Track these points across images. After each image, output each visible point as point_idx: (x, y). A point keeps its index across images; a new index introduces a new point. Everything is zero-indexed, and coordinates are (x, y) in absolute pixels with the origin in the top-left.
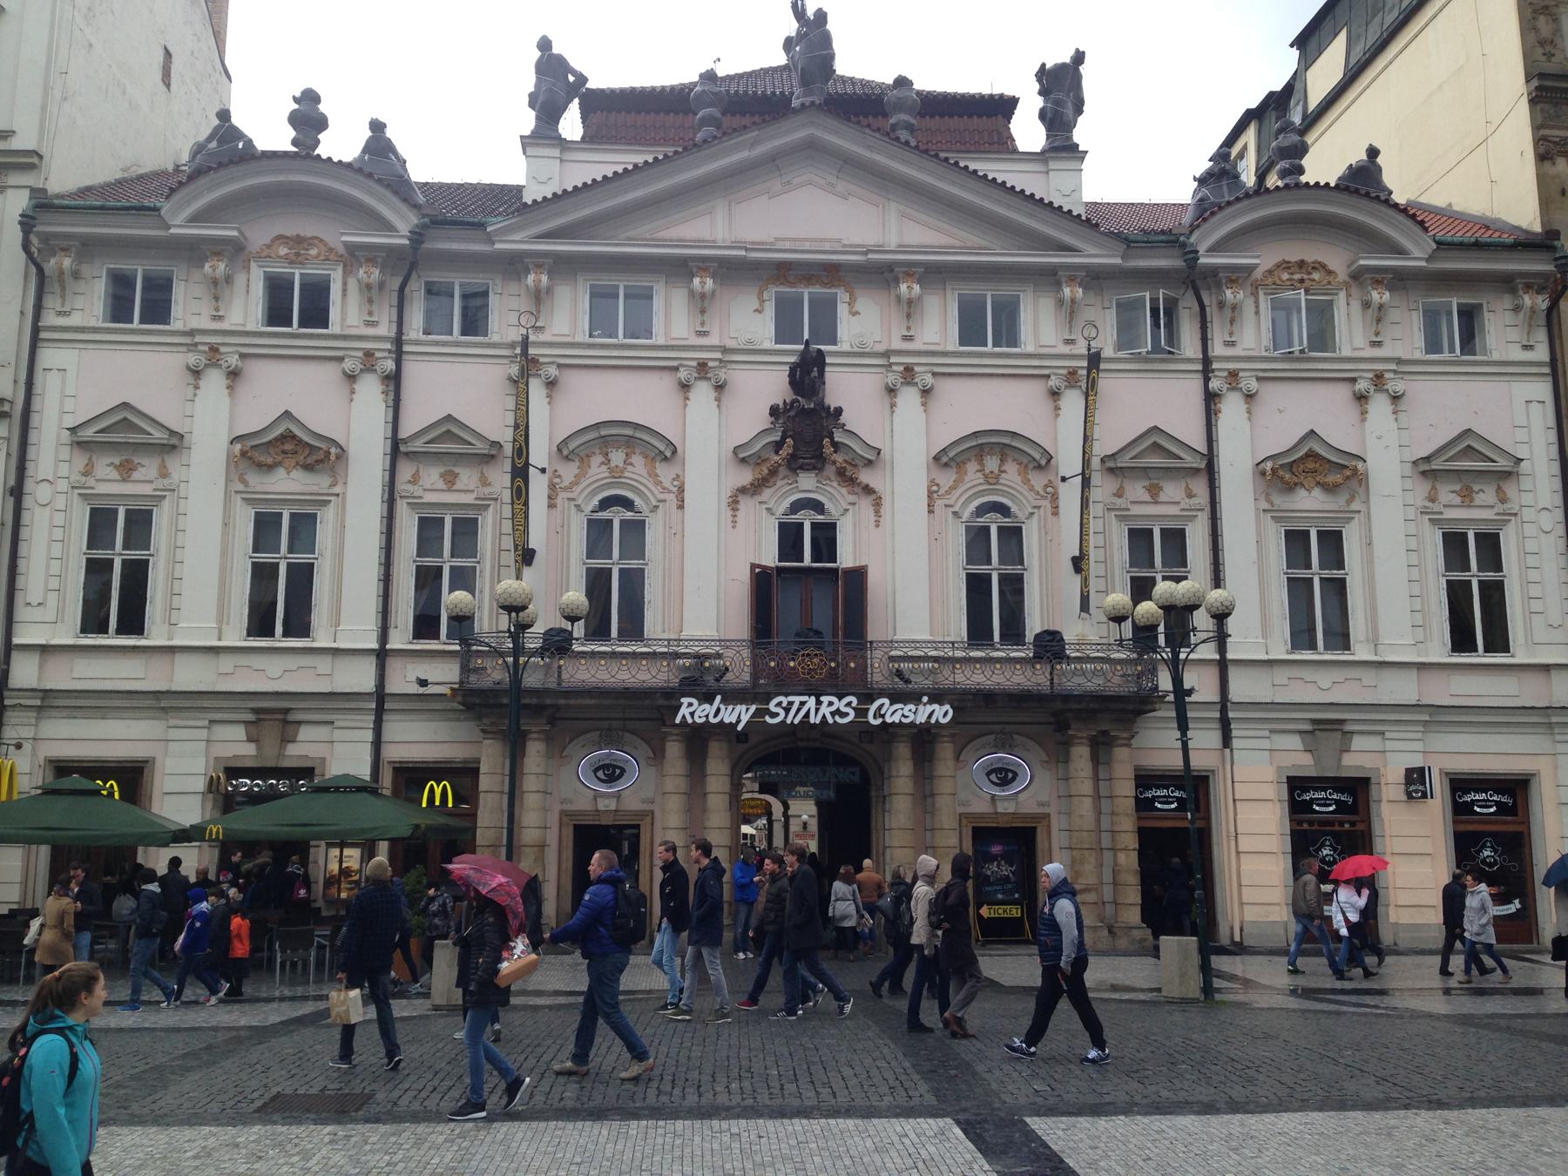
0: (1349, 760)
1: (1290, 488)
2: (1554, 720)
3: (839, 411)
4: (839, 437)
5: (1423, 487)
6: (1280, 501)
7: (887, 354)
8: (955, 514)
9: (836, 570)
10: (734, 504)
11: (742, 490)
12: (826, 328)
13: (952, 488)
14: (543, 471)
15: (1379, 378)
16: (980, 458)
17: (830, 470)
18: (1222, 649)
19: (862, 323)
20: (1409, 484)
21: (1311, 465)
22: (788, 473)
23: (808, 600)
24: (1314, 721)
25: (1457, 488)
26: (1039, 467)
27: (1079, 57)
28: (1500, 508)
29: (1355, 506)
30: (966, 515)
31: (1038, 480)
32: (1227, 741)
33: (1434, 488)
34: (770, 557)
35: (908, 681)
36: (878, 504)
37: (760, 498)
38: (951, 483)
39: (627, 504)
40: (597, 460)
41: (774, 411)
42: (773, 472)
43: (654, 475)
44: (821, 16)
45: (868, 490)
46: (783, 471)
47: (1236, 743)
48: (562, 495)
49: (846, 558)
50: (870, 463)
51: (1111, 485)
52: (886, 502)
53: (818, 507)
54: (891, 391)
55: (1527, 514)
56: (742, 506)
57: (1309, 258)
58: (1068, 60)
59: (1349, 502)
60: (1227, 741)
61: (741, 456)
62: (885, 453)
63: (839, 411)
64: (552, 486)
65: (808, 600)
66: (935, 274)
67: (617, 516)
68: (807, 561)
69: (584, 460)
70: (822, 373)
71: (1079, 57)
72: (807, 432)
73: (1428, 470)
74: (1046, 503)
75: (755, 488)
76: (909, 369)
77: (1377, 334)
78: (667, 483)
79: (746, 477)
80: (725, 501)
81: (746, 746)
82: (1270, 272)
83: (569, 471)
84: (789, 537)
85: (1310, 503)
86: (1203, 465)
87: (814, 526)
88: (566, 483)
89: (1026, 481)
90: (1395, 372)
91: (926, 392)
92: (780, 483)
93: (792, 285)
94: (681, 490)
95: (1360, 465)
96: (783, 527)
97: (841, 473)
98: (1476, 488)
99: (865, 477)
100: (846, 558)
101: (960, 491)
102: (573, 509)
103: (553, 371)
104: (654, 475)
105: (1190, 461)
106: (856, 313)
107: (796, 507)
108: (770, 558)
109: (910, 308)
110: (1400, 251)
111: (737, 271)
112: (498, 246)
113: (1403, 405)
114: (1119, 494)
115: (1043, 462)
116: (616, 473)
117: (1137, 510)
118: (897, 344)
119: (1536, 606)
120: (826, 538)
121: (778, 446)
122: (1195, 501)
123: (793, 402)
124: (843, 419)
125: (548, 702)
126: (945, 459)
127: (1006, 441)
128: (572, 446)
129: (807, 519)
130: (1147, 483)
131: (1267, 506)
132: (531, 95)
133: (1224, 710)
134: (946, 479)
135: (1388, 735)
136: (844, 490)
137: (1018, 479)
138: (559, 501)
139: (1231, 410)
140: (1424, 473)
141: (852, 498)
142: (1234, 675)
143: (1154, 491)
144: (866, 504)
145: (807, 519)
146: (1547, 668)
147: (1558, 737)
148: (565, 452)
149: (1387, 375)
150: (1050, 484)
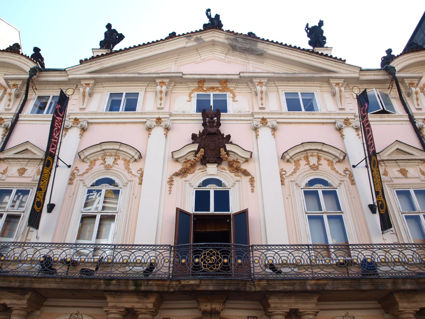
3: (229, 137)
4: (229, 147)
7: (252, 114)
8: (297, 184)
9: (229, 216)
10: (171, 181)
11: (177, 174)
12: (221, 107)
13: (294, 172)
14: (69, 166)
16: (306, 158)
17: (224, 165)
19: (239, 104)
22: (202, 167)
26: (339, 161)
27: (321, 23)
30: (303, 185)
31: (340, 168)
34: (190, 207)
35: (280, 272)
36: (252, 180)
37: (184, 179)
38: (292, 170)
39: (111, 182)
40: (98, 163)
41: (194, 136)
42: (193, 166)
44: (217, 16)
45: (246, 173)
46: (199, 166)
49: (235, 208)
50: (247, 160)
53: (218, 183)
54: (256, 129)
61: (176, 157)
62: (255, 155)
63: (229, 137)
64: (73, 174)
66: (274, 80)
67: (105, 188)
68: (212, 210)
69: (93, 163)
70: (219, 119)
71: (321, 23)
72: (211, 144)
74: (347, 179)
75: (183, 173)
76: (264, 121)
78: (134, 172)
79: (178, 167)
80: (166, 179)
83: (83, 167)
84: (201, 198)
87: (215, 192)
88: (81, 173)
89: (334, 169)
91: (274, 129)
92: (196, 172)
94: (142, 175)
96: (198, 193)
97: (231, 165)
99: (244, 166)
100: (235, 208)
102: (82, 185)
103: (85, 124)
104: (128, 168)
106: (236, 101)
107: (206, 183)
108: (190, 207)
109: (263, 96)
111: (177, 80)
112: (70, 76)
115: (341, 158)
116: (108, 168)
117: (396, 181)
118: (257, 110)
120: (223, 198)
121: (197, 152)
123: (204, 131)
124: (232, 139)
125: (27, 285)
126: (288, 157)
127: (319, 148)
128: (86, 153)
129: (212, 189)
132: (101, 42)
134: (289, 168)
136: (233, 175)
137: (329, 168)
138: (75, 181)
141: (238, 178)
144: (246, 180)
145: (212, 189)
148: (82, 157)
150: (346, 170)
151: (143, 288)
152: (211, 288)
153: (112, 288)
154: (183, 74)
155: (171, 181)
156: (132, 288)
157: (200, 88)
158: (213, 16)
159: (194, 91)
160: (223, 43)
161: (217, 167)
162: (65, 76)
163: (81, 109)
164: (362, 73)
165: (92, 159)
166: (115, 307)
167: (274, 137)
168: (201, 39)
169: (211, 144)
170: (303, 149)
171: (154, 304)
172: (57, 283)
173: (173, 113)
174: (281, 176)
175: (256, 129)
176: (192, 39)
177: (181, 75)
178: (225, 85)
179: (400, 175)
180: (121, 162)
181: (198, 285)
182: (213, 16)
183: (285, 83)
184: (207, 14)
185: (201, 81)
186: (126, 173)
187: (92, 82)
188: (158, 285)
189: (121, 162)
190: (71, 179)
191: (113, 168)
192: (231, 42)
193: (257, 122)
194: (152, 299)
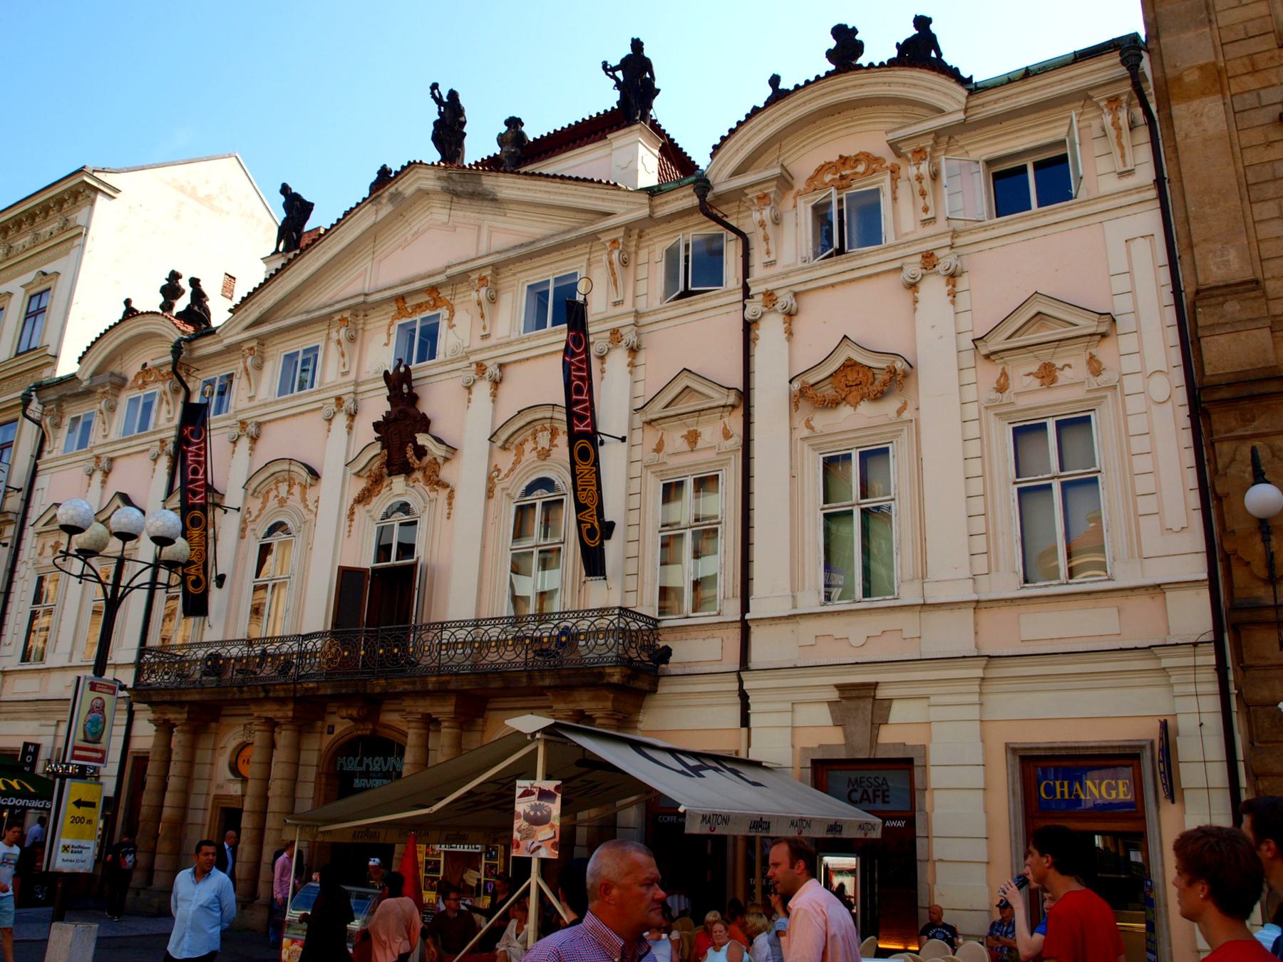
0: (888, 736)
1: (834, 404)
2: (1165, 663)
4: (422, 439)
5: (991, 373)
6: (825, 421)
13: (512, 470)
14: (238, 510)
15: (929, 259)
17: (418, 475)
18: (745, 608)
20: (970, 376)
21: (852, 376)
23: (383, 593)
24: (840, 687)
25: (1034, 368)
28: (1095, 382)
29: (906, 415)
32: (745, 721)
33: (1004, 374)
36: (451, 497)
37: (368, 507)
43: (304, 500)
47: (754, 720)
48: (250, 527)
50: (446, 459)
51: (652, 437)
52: (457, 494)
55: (1131, 384)
56: (356, 517)
57: (850, 151)
58: (629, 51)
59: (899, 412)
60: (745, 721)
64: (244, 521)
65: (383, 593)
73: (986, 350)
75: (363, 498)
76: (481, 367)
77: (926, 210)
80: (346, 511)
81: (332, 736)
82: (812, 179)
83: (255, 505)
85: (853, 423)
86: (732, 399)
90: (952, 247)
93: (410, 315)
95: (899, 365)
98: (1059, 364)
101: (516, 471)
105: (720, 398)
110: (940, 112)
113: (962, 283)
114: (659, 448)
116: (282, 502)
118: (478, 344)
119: (1145, 505)
122: (731, 442)
128: (254, 484)
130: (685, 433)
131: (806, 433)
133: (741, 682)
134: (505, 460)
135: (933, 700)
136: (427, 488)
139: (770, 331)
140: (987, 357)
141: (433, 495)
142: (756, 634)
143: (693, 438)
144: (444, 494)
146: (1158, 588)
147: (1177, 689)
149: (937, 254)
151: (271, 695)
152: (329, 692)
153: (245, 696)
154: (366, 295)
155: (352, 513)
156: (262, 695)
157: (401, 312)
158: (445, 100)
159: (394, 318)
160: (435, 192)
161: (406, 480)
162: (217, 342)
163: (251, 398)
164: (658, 200)
165: (264, 491)
166: (259, 717)
167: (493, 401)
168: (400, 193)
169: (403, 437)
170: (522, 423)
171: (294, 710)
172: (200, 694)
173: (364, 377)
174: (490, 479)
175: (469, 388)
176: (384, 201)
177: (361, 299)
178: (435, 295)
179: (686, 447)
180: (297, 490)
181: (318, 689)
182: (445, 100)
183: (527, 264)
184: (433, 96)
185: (401, 299)
186: (301, 507)
187: (254, 344)
188: (284, 690)
189: (297, 490)
190: (243, 530)
191: (289, 503)
192: (445, 184)
193: (472, 374)
194: (291, 706)
